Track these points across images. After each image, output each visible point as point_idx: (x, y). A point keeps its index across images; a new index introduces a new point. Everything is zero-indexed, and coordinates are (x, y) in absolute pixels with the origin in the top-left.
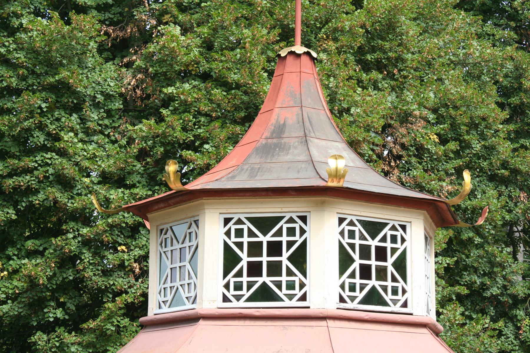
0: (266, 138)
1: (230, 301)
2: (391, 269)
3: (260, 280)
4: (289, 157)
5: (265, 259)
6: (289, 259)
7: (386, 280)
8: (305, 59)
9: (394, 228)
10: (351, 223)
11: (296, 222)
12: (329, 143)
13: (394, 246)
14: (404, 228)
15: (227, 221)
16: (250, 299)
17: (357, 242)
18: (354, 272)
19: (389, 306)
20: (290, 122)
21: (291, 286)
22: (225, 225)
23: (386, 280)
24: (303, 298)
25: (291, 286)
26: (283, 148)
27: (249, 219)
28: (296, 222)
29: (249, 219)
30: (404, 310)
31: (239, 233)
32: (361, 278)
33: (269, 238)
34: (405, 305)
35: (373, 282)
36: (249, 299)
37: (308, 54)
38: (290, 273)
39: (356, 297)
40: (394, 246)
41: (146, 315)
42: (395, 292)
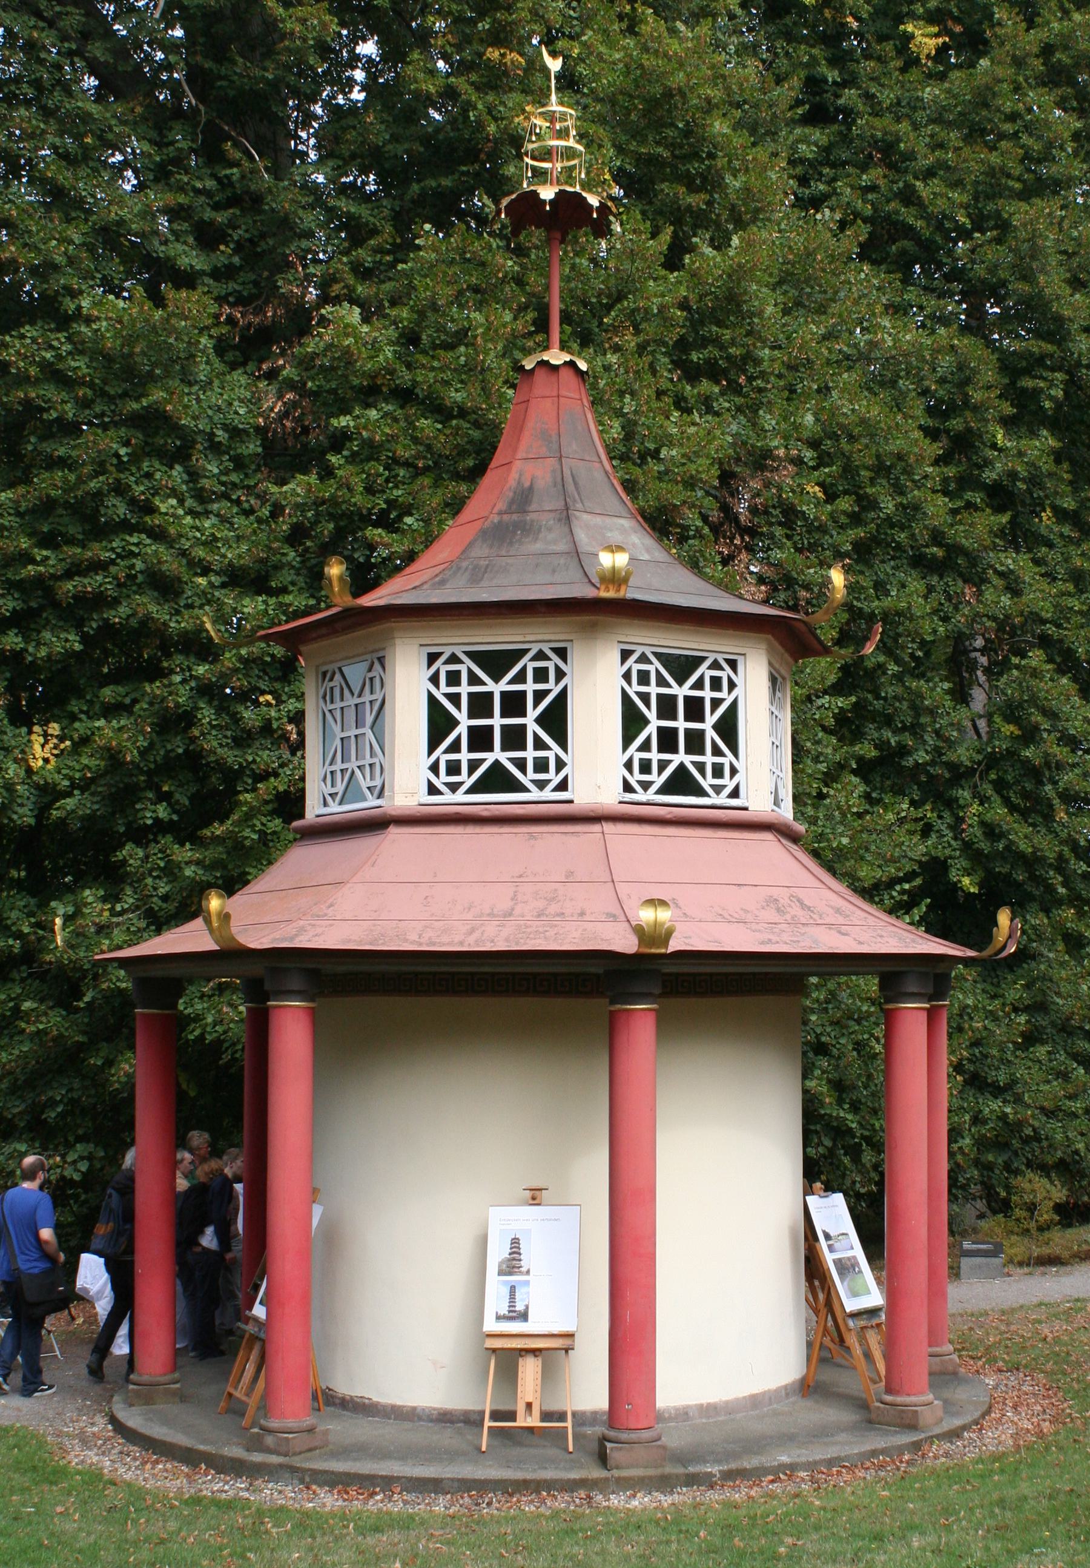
0: (500, 513)
1: (439, 793)
2: (711, 734)
3: (490, 758)
4: (538, 546)
5: (497, 722)
7: (702, 752)
8: (566, 375)
9: (716, 665)
10: (643, 659)
11: (549, 659)
12: (608, 521)
13: (717, 695)
14: (733, 664)
15: (432, 658)
17: (653, 690)
18: (648, 740)
19: (708, 796)
20: (540, 484)
21: (541, 766)
22: (430, 665)
23: (702, 752)
24: (563, 786)
25: (541, 766)
26: (528, 530)
27: (469, 654)
28: (549, 659)
30: (734, 802)
31: (454, 678)
32: (661, 750)
33: (504, 685)
34: (735, 793)
35: (681, 757)
36: (471, 791)
37: (571, 364)
38: (539, 744)
39: (652, 783)
40: (717, 695)
41: (302, 816)
42: (718, 771)
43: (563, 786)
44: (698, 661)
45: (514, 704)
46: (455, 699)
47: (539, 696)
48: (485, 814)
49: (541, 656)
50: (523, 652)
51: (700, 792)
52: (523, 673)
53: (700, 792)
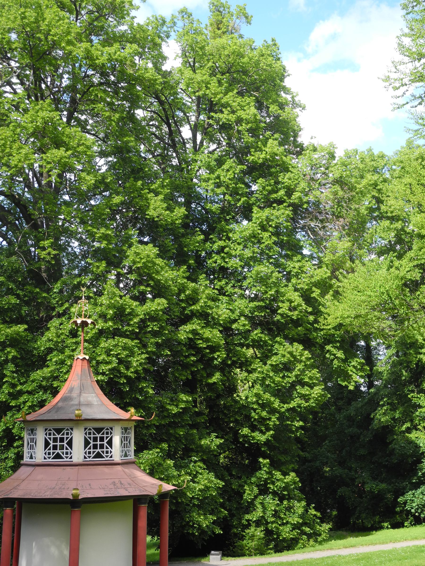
6: (67, 443)
15: (46, 430)
21: (67, 453)
24: (71, 458)
25: (67, 453)
27: (53, 429)
36: (53, 459)
38: (67, 449)
45: (62, 440)
46: (50, 439)
49: (68, 430)
52: (64, 433)
53: (103, 457)
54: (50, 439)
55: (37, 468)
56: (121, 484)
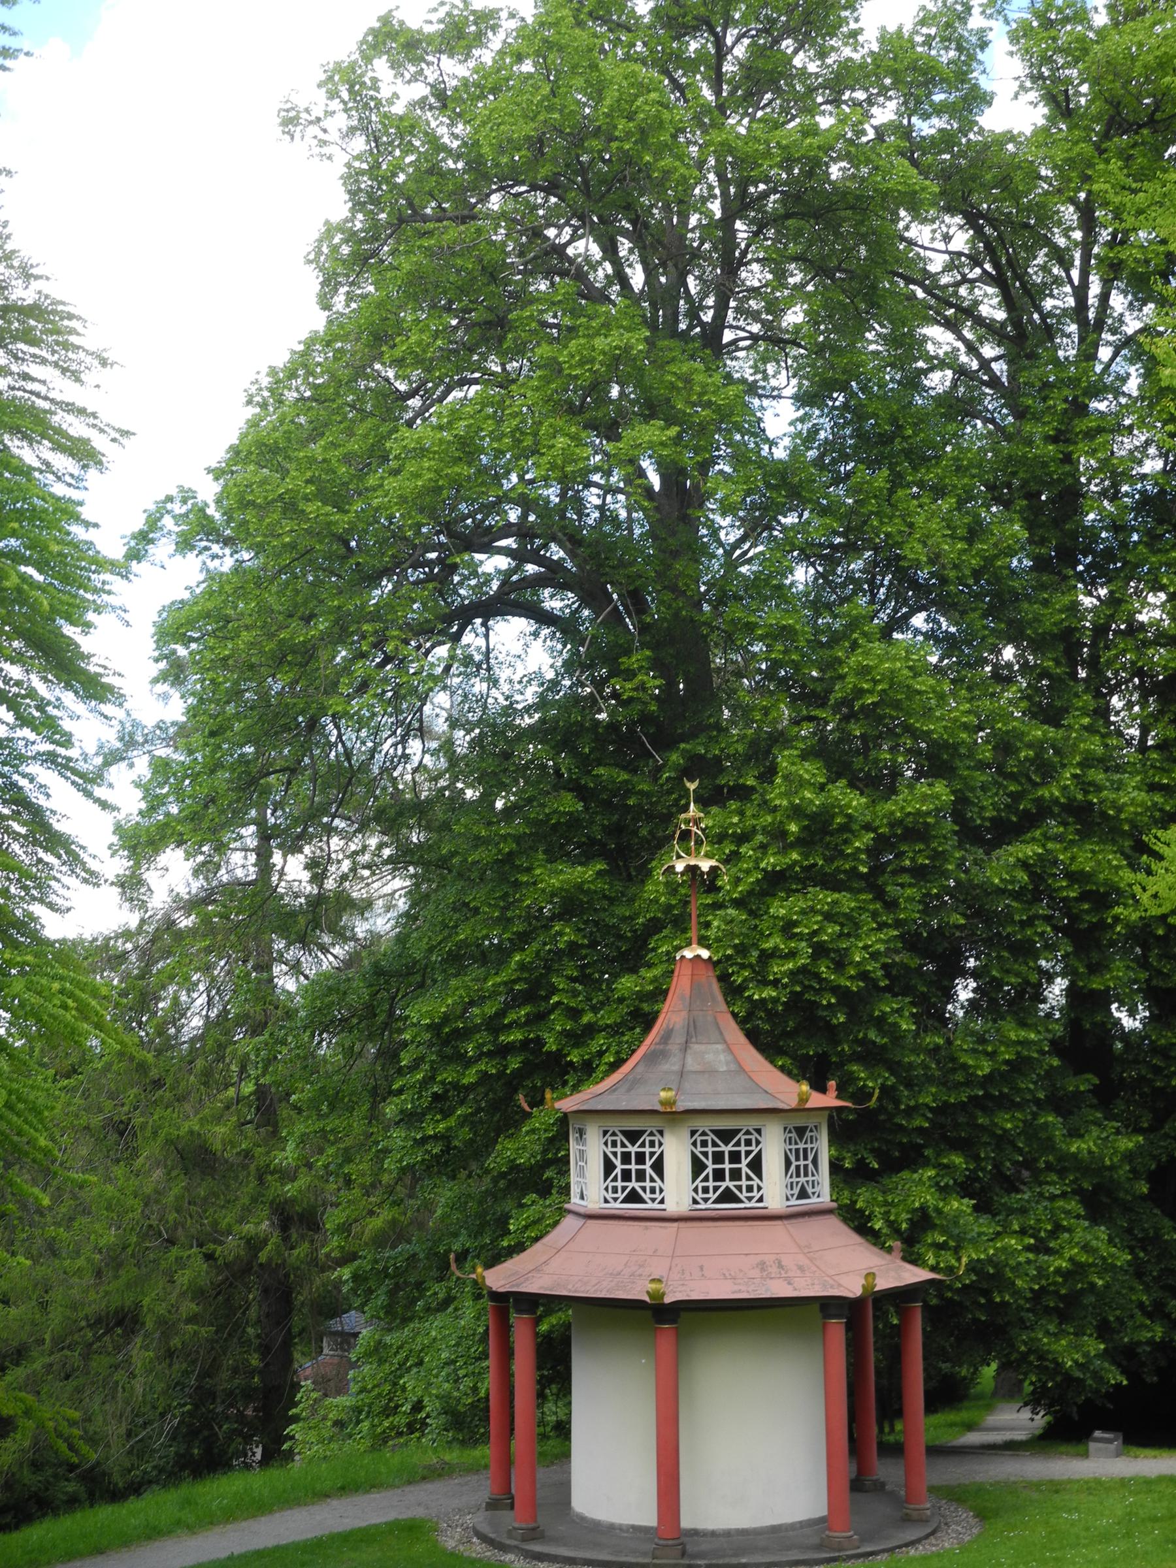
3: (724, 1185)
5: (727, 1166)
6: (748, 1166)
15: (693, 1133)
16: (716, 1201)
21: (750, 1189)
24: (761, 1200)
25: (750, 1189)
27: (713, 1131)
29: (713, 1131)
31: (704, 1144)
33: (730, 1148)
36: (715, 1202)
38: (749, 1178)
43: (761, 1200)
44: (642, 1133)
45: (735, 1157)
47: (748, 1153)
48: (714, 1213)
49: (748, 1133)
50: (738, 1131)
51: (642, 1201)
54: (615, 1154)
55: (591, 1222)
56: (781, 1266)
